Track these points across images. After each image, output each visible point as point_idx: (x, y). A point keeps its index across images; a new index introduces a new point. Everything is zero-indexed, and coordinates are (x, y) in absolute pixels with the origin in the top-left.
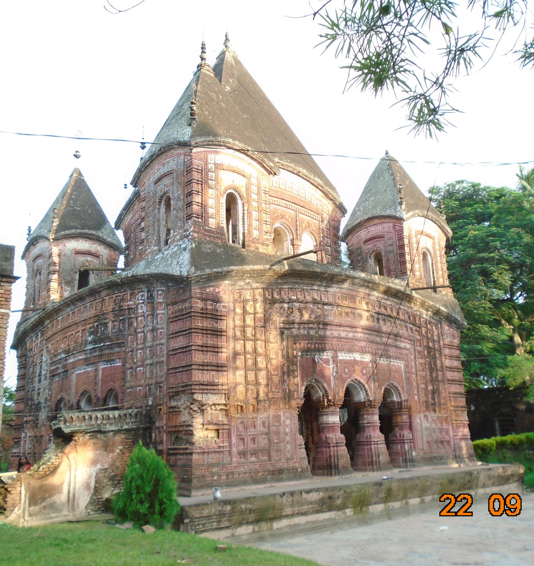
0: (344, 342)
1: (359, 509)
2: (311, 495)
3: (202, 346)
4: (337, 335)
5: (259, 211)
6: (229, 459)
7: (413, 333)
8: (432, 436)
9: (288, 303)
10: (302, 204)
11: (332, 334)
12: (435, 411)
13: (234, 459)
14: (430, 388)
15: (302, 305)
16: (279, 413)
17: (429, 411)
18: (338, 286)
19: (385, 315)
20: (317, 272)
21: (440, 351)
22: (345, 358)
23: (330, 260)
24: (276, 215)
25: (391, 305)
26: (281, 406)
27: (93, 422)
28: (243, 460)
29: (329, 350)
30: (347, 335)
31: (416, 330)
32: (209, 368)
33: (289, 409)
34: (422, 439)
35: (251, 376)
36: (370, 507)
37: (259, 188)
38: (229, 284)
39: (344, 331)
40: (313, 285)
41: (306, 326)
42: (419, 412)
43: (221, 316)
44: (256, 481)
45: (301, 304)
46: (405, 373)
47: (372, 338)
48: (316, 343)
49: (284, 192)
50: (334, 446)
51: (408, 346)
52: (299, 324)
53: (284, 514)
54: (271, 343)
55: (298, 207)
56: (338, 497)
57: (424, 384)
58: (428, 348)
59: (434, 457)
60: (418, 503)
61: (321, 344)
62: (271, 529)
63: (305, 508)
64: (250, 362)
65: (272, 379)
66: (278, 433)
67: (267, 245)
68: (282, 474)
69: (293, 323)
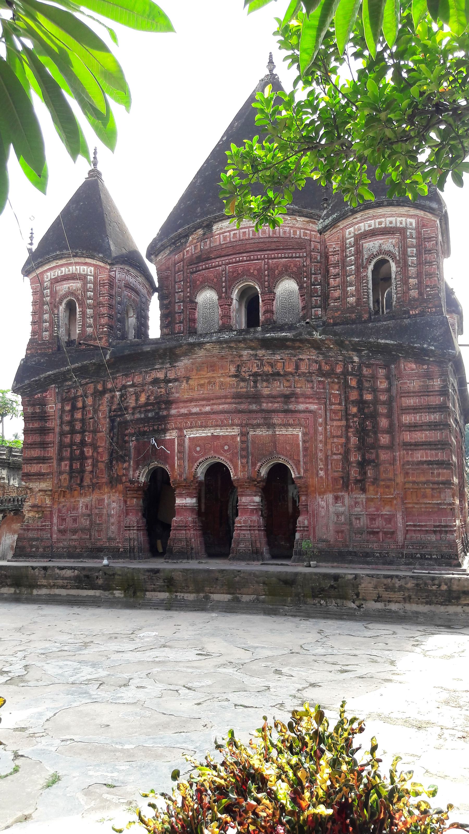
0: (193, 418)
1: (131, 592)
2: (64, 571)
3: (31, 444)
4: (186, 412)
5: (93, 307)
6: (49, 535)
7: (324, 388)
8: (351, 524)
9: (120, 390)
10: (273, 247)
11: (178, 412)
12: (364, 490)
13: (55, 536)
14: (355, 457)
15: (139, 389)
16: (103, 497)
17: (347, 490)
18: (188, 357)
19: (267, 375)
20: (148, 352)
21: (389, 402)
22: (198, 435)
23: (319, 302)
24: (235, 274)
25: (282, 359)
26: (106, 490)
27: (16, 503)
28: (64, 537)
29: (173, 429)
30: (200, 410)
31: (333, 382)
32: (35, 461)
33: (115, 492)
34: (327, 526)
35: (76, 465)
36: (147, 593)
37: (95, 283)
38: (55, 387)
39: (195, 406)
40: (154, 364)
41: (142, 409)
42: (324, 493)
43: (49, 416)
44: (71, 556)
45: (136, 388)
46: (304, 442)
47: (243, 407)
48: (154, 425)
49: (246, 242)
50: (174, 530)
51: (313, 407)
52: (134, 408)
53: (38, 583)
54: (100, 432)
55: (268, 252)
56: (97, 578)
57: (340, 454)
58: (361, 403)
59: (350, 553)
60: (226, 600)
61: (159, 425)
62: (31, 594)
63: (60, 582)
64: (78, 452)
65: (97, 466)
66: (100, 516)
67: (100, 339)
68: (101, 552)
69: (126, 409)
